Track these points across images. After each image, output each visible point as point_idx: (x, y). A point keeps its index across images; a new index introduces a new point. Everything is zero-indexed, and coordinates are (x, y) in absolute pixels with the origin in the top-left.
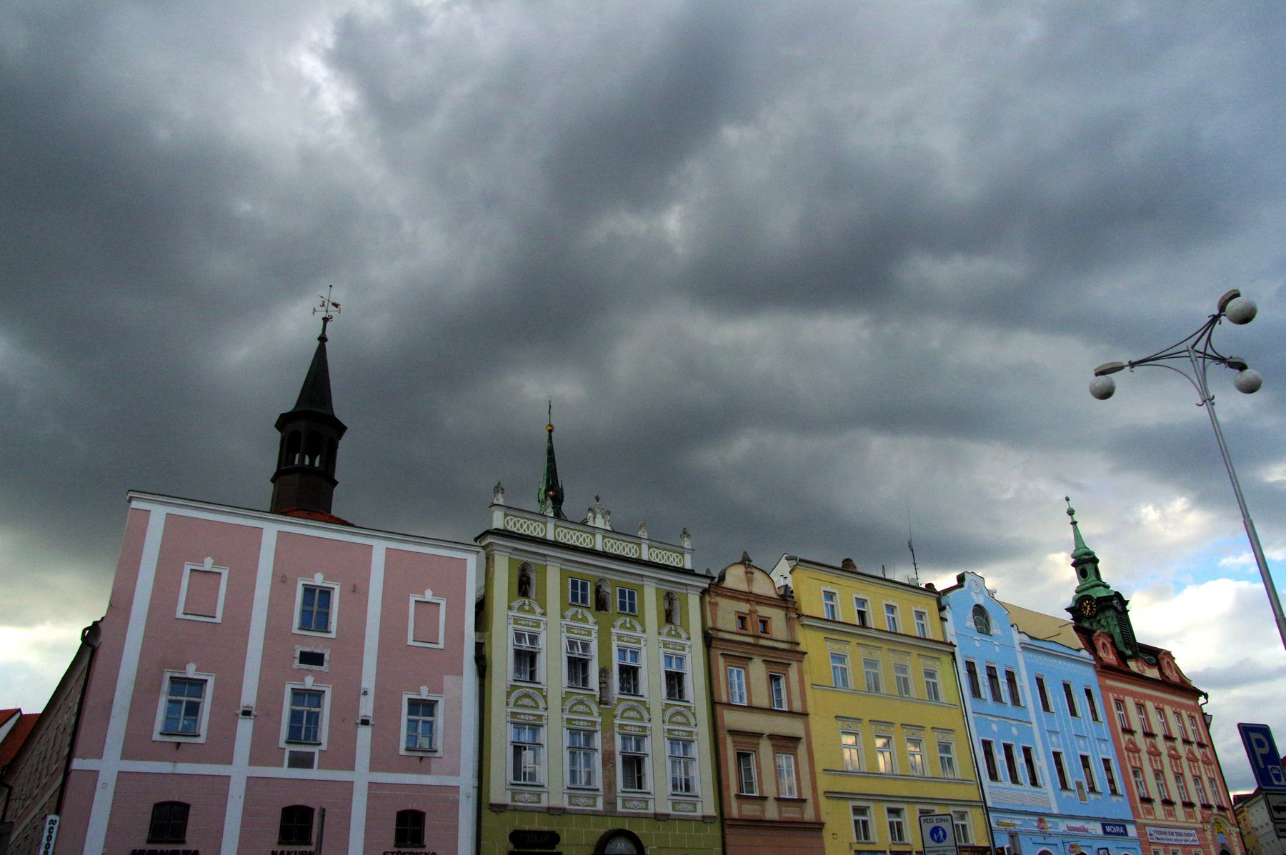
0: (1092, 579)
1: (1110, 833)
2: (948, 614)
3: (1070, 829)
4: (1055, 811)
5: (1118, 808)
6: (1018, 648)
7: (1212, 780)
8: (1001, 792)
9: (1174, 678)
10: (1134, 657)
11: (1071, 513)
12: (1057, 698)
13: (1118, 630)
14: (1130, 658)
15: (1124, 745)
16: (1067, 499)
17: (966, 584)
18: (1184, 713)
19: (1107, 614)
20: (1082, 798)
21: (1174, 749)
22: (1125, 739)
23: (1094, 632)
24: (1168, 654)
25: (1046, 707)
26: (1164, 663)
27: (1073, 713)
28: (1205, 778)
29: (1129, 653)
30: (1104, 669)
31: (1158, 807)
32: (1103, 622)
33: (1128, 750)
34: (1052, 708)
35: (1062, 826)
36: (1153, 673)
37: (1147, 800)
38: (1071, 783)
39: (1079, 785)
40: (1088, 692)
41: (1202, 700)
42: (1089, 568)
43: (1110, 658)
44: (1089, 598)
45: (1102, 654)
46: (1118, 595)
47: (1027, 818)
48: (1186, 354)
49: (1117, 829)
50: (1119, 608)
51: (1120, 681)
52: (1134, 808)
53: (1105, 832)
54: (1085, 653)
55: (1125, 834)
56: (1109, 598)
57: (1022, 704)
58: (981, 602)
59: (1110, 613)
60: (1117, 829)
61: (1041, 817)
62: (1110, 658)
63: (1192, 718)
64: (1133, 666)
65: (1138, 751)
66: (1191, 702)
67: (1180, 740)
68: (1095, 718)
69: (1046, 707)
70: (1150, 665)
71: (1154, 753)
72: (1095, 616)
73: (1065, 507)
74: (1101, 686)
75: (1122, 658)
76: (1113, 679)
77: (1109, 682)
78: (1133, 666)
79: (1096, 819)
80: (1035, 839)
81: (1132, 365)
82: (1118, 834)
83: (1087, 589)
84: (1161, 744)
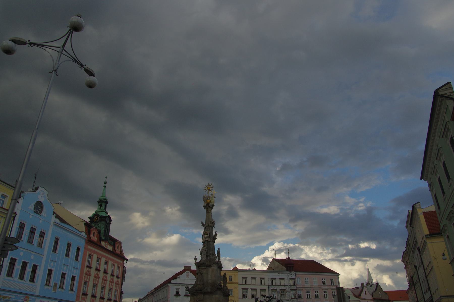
0: (103, 208)
2: (21, 201)
4: (37, 293)
6: (52, 224)
7: (116, 291)
9: (118, 251)
10: (105, 240)
11: (105, 183)
12: (62, 248)
13: (103, 229)
14: (103, 240)
15: (85, 272)
16: (106, 178)
17: (37, 191)
18: (116, 265)
19: (102, 222)
20: (55, 290)
21: (106, 277)
22: (86, 269)
23: (92, 227)
24: (120, 243)
25: (55, 250)
26: (117, 246)
27: (67, 255)
28: (114, 290)
29: (103, 238)
30: (89, 241)
31: (89, 298)
32: (99, 225)
33: (86, 274)
34: (57, 252)
36: (110, 248)
37: (85, 295)
38: (52, 283)
39: (55, 285)
40: (78, 249)
41: (125, 262)
42: (103, 204)
43: (94, 238)
44: (98, 215)
45: (92, 236)
46: (109, 217)
47: (19, 295)
48: (58, 49)
50: (108, 222)
51: (94, 247)
54: (84, 234)
56: (105, 217)
57: (43, 247)
58: (42, 200)
59: (103, 222)
62: (94, 238)
63: (119, 267)
64: (103, 244)
65: (90, 275)
66: (121, 262)
67: (110, 274)
68: (77, 259)
69: (55, 250)
70: (110, 245)
71: (97, 277)
72: (98, 222)
73: (104, 180)
74: (85, 248)
75: (100, 240)
76: (90, 246)
77: (89, 247)
78: (103, 244)
81: (32, 44)
83: (99, 212)
84: (101, 274)
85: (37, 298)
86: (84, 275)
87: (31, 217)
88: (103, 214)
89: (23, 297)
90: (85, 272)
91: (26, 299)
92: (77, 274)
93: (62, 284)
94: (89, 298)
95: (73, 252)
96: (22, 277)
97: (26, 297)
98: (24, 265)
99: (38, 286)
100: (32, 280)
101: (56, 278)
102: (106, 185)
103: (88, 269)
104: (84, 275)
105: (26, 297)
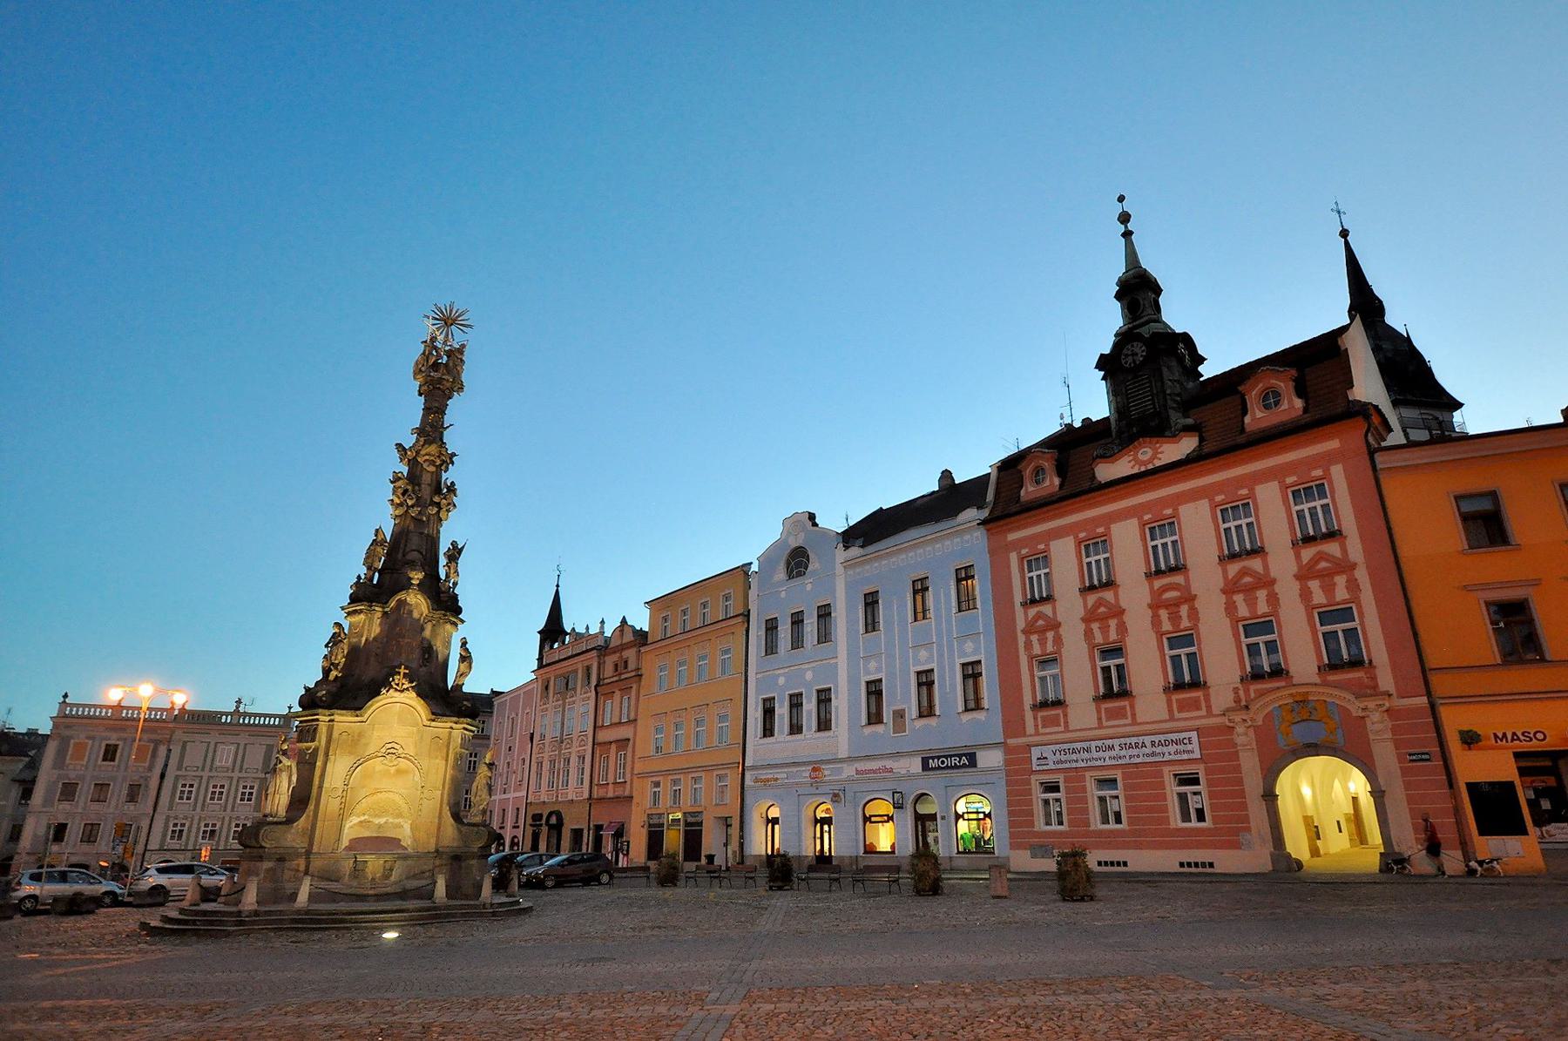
1: (939, 768)
3: (858, 772)
4: (843, 754)
8: (783, 744)
11: (1125, 218)
15: (1021, 624)
25: (871, 625)
31: (1082, 710)
35: (849, 771)
52: (1012, 724)
53: (925, 767)
60: (955, 761)
69: (871, 625)
76: (1010, 530)
77: (1012, 537)
78: (1106, 471)
79: (910, 754)
82: (956, 767)
86: (1021, 639)
87: (783, 595)
90: (1021, 624)
92: (983, 650)
93: (873, 710)
95: (943, 596)
96: (796, 728)
98: (796, 702)
99: (841, 737)
100: (824, 725)
101: (902, 696)
103: (1032, 612)
104: (1021, 639)
105: (814, 770)
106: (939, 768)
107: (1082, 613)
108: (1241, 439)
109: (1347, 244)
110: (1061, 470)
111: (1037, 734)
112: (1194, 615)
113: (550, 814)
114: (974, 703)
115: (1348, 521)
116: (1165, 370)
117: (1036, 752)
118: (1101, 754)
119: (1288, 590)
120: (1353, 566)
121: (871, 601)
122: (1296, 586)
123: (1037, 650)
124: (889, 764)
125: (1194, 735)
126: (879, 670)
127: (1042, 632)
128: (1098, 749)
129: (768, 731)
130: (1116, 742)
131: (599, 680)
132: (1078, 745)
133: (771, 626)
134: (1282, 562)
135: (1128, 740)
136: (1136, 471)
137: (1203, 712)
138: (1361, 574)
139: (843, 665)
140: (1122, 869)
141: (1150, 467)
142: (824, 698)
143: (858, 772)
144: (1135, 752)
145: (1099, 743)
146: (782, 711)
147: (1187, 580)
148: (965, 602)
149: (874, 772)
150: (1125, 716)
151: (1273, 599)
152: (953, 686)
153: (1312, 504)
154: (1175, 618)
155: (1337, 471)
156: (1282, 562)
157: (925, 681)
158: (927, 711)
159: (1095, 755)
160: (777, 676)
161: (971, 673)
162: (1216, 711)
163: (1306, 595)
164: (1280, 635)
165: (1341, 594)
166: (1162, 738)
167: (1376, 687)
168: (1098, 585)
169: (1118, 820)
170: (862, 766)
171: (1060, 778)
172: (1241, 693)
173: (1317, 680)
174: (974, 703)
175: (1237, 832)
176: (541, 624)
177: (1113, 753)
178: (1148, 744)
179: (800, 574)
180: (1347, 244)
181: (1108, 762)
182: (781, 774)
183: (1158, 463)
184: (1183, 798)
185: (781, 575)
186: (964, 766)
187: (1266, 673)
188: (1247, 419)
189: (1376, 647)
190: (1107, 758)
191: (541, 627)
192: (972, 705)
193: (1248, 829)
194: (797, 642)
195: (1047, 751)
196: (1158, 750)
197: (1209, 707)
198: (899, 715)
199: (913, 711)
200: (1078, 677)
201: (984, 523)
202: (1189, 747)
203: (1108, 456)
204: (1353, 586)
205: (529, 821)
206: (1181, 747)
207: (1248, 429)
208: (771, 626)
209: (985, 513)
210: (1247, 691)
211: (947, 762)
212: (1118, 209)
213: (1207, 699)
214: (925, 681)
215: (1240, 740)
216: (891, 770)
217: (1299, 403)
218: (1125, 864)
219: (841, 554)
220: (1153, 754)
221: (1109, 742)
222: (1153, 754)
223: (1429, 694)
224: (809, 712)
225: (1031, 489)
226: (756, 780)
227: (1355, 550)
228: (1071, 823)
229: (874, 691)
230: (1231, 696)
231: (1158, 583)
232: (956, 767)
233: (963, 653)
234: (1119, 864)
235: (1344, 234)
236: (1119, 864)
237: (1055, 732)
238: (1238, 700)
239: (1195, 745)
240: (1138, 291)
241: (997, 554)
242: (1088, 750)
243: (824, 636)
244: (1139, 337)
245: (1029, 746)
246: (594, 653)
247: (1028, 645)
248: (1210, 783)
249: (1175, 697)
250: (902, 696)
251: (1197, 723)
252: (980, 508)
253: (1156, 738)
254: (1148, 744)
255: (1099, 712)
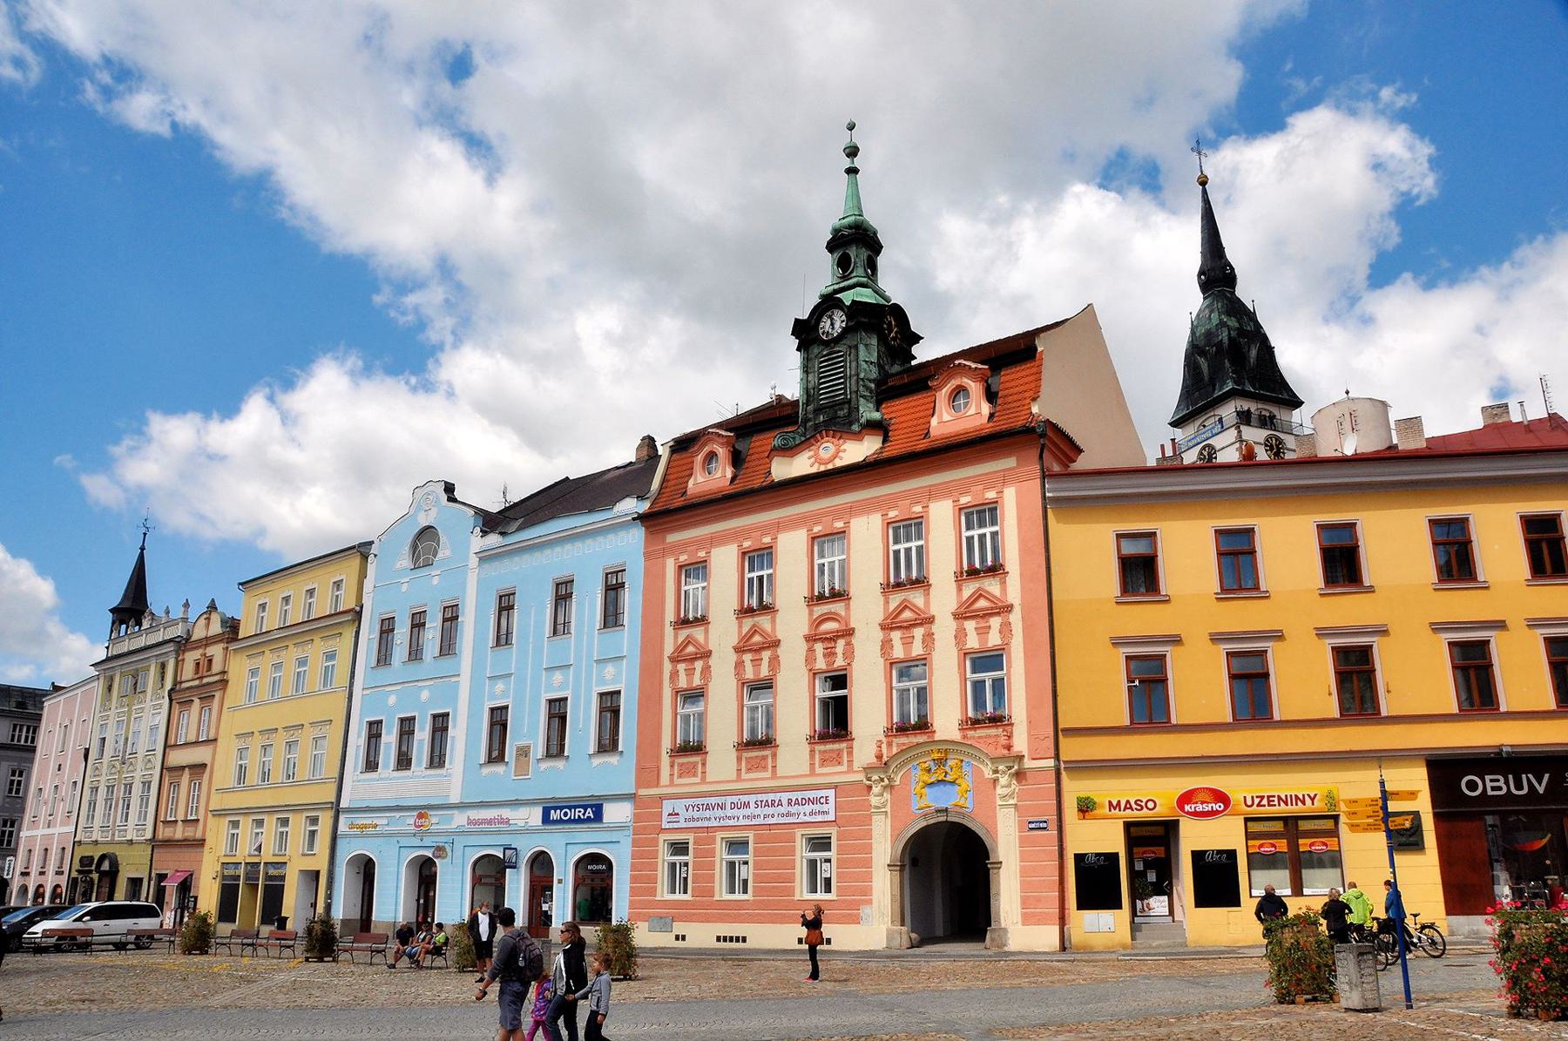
0: (859, 274)
1: (561, 821)
3: (470, 822)
4: (455, 798)
5: (613, 774)
6: (474, 561)
8: (388, 784)
11: (852, 152)
15: (669, 648)
20: (522, 769)
25: (503, 639)
31: (722, 760)
35: (460, 819)
47: (398, 815)
49: (579, 813)
52: (647, 772)
53: (546, 819)
55: (598, 817)
60: (579, 813)
61: (422, 811)
69: (503, 639)
74: (647, 556)
80: (405, 842)
82: (579, 821)
85: (455, 812)
87: (404, 588)
88: (865, 296)
89: (410, 818)
91: (420, 822)
92: (624, 679)
94: (722, 760)
95: (588, 604)
96: (404, 762)
97: (420, 816)
100: (437, 759)
101: (529, 730)
102: (847, 163)
105: (420, 816)
106: (561, 821)
107: (735, 640)
108: (923, 445)
109: (1205, 192)
110: (737, 459)
111: (672, 784)
112: (849, 653)
113: (103, 857)
114: (608, 744)
115: (1012, 558)
116: (861, 347)
117: (668, 806)
118: (736, 812)
119: (945, 628)
120: (1009, 608)
121: (505, 605)
122: (952, 625)
123: (683, 683)
124: (506, 813)
125: (831, 793)
126: (505, 694)
127: (692, 659)
128: (734, 806)
129: (371, 765)
130: (752, 799)
131: (176, 683)
132: (713, 801)
133: (387, 628)
134: (943, 597)
135: (764, 797)
136: (814, 470)
137: (844, 768)
138: (1015, 618)
139: (465, 688)
140: (740, 945)
141: (830, 466)
142: (440, 724)
143: (470, 822)
144: (770, 810)
145: (735, 799)
146: (390, 738)
147: (848, 608)
148: (612, 617)
149: (490, 822)
150: (765, 768)
151: (929, 639)
152: (587, 719)
153: (908, 545)
154: (830, 654)
155: (1010, 496)
156: (943, 597)
157: (558, 713)
158: (556, 748)
159: (729, 813)
160: (390, 695)
161: (610, 705)
162: (856, 765)
163: (960, 636)
164: (1009, 673)
165: (994, 639)
166: (799, 795)
167: (1009, 747)
168: (829, 596)
169: (828, 890)
170: (475, 814)
171: (690, 838)
172: (884, 746)
173: (956, 735)
174: (608, 744)
175: (856, 905)
176: (115, 596)
177: (747, 812)
178: (785, 802)
179: (428, 564)
180: (1205, 192)
181: (742, 822)
182: (381, 820)
183: (839, 463)
184: (813, 864)
185: (405, 562)
186: (589, 820)
187: (912, 725)
188: (934, 421)
189: (1018, 705)
190: (740, 817)
191: (115, 601)
192: (554, 750)
193: (870, 902)
194: (415, 653)
195: (679, 806)
196: (793, 809)
197: (850, 762)
198: (523, 752)
199: (539, 749)
200: (723, 720)
201: (642, 518)
202: (825, 808)
203: (789, 450)
204: (1006, 629)
205: (76, 865)
206: (816, 807)
207: (933, 433)
208: (387, 628)
209: (644, 507)
210: (890, 745)
211: (571, 814)
212: (845, 139)
213: (850, 753)
214: (558, 713)
215: (874, 800)
216: (507, 821)
217: (986, 408)
218: (744, 940)
219: (478, 542)
220: (789, 814)
221: (745, 798)
222: (789, 814)
223: (1057, 757)
224: (421, 741)
225: (700, 479)
226: (352, 826)
227: (1014, 594)
228: (757, 892)
229: (499, 721)
230: (873, 750)
231: (820, 610)
232: (579, 821)
233: (602, 681)
234: (737, 939)
235: (1203, 183)
236: (737, 939)
237: (690, 784)
238: (879, 757)
239: (831, 806)
240: (855, 244)
241: (652, 556)
242: (722, 807)
243: (448, 647)
244: (839, 304)
245: (662, 798)
246: (171, 647)
247: (674, 675)
248: (757, 852)
249: (819, 748)
250: (529, 730)
251: (837, 779)
252: (641, 498)
253: (794, 796)
254: (785, 802)
255: (739, 759)
